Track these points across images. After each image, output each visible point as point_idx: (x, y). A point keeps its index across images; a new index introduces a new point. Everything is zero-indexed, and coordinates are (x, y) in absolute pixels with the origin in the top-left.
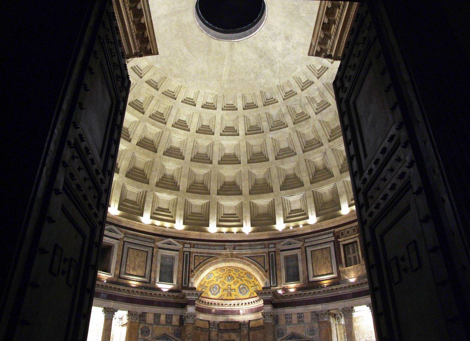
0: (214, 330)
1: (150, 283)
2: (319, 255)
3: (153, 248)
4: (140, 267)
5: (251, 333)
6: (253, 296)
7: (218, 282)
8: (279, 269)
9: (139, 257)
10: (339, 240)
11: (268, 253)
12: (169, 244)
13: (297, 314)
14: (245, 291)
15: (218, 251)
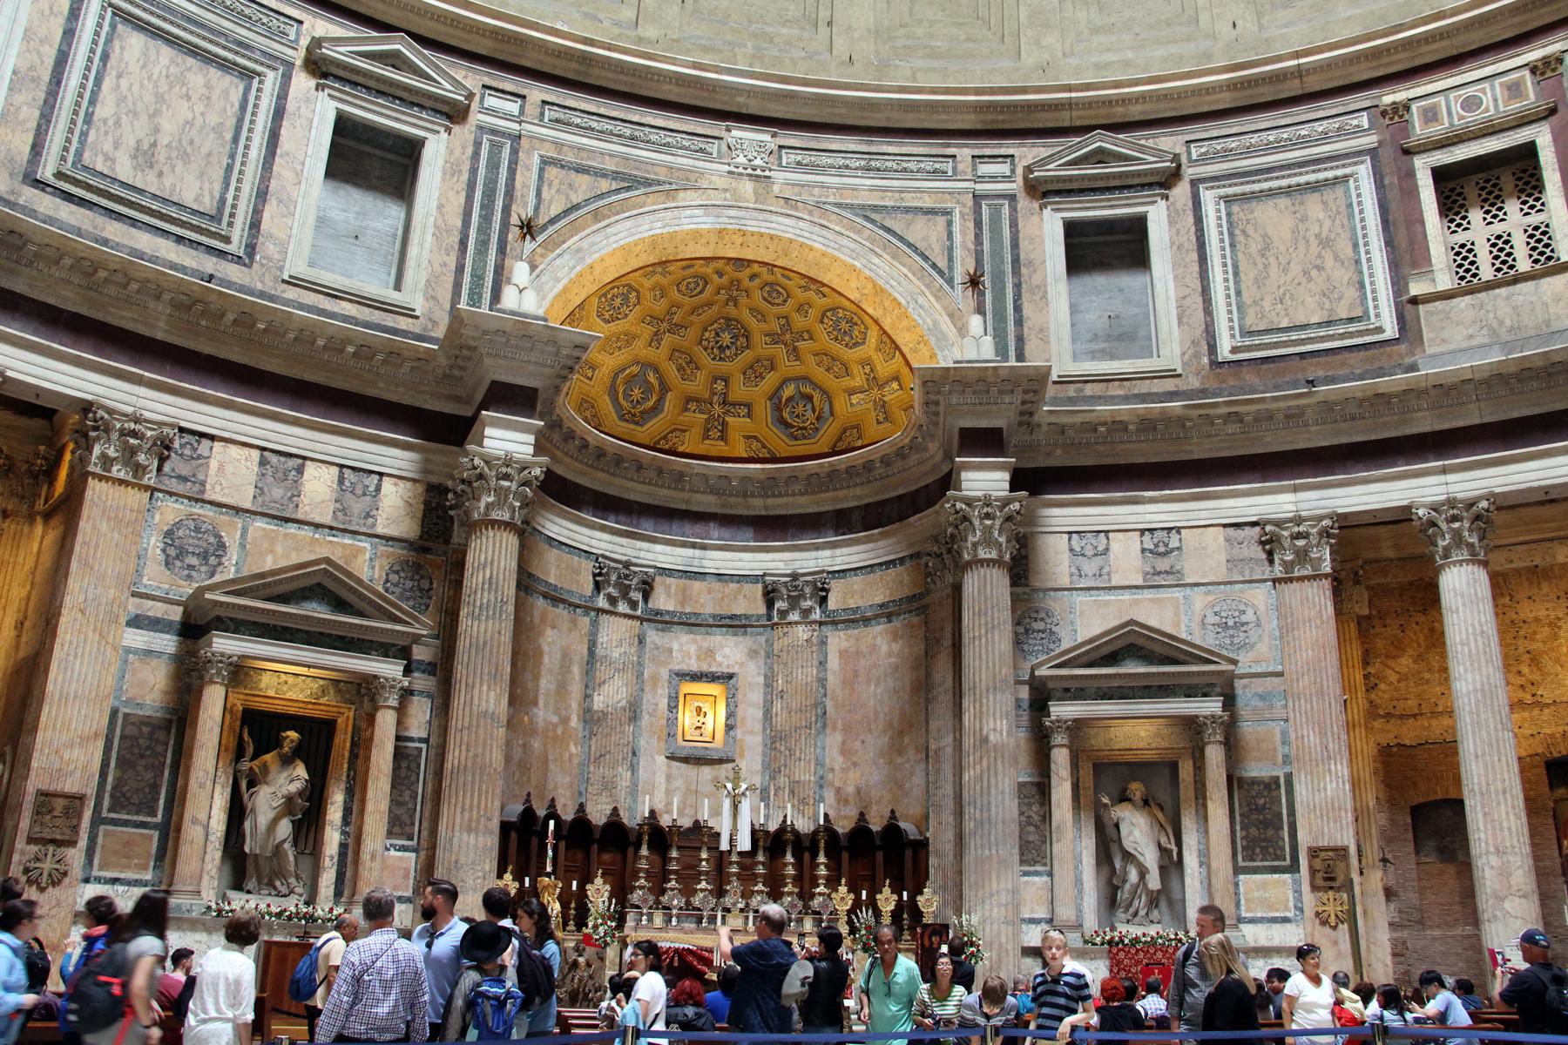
0: (623, 607)
1: (245, 265)
2: (1273, 218)
3: (289, 65)
4: (185, 152)
5: (838, 640)
6: (859, 443)
7: (659, 354)
8: (1038, 287)
9: (189, 98)
10: (1411, 142)
11: (971, 203)
12: (393, 60)
13: (1142, 535)
14: (809, 414)
15: (683, 162)
